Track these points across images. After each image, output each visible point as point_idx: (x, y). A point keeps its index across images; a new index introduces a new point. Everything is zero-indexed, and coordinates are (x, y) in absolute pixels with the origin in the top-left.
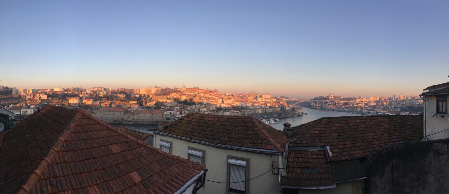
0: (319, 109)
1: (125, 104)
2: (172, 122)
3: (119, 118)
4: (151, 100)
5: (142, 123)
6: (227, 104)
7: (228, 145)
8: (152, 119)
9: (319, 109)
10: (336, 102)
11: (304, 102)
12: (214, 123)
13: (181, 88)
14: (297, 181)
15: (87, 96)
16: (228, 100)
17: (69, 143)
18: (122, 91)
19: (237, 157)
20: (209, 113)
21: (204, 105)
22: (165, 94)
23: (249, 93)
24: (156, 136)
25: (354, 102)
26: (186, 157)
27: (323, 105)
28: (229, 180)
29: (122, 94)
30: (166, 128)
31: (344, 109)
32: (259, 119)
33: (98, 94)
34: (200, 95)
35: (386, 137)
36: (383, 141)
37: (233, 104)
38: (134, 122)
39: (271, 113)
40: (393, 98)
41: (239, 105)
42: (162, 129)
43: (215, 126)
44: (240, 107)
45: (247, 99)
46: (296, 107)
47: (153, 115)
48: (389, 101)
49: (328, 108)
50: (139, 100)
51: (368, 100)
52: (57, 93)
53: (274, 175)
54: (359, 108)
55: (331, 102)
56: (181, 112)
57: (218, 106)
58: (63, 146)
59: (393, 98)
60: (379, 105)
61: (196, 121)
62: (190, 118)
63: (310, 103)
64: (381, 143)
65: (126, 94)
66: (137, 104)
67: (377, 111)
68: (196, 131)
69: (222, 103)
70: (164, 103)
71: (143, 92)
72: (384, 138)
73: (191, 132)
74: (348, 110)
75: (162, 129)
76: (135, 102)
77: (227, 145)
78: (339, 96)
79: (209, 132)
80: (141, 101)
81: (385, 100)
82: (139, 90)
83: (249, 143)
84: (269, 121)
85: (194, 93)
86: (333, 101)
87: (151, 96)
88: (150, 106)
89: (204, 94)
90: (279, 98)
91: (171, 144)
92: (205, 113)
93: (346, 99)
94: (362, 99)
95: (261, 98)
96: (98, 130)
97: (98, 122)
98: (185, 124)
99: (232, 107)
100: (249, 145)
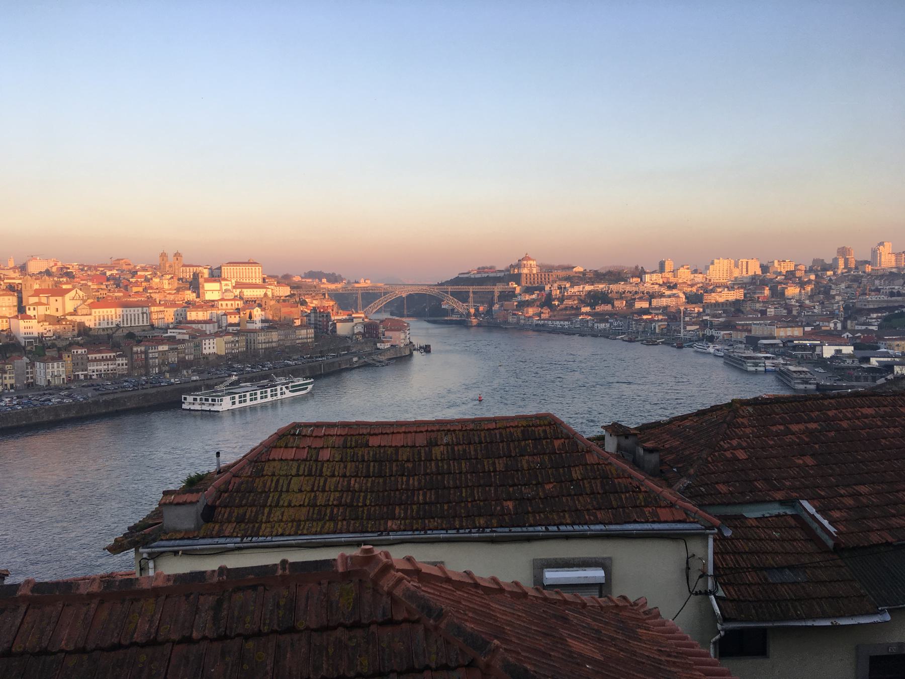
0: (479, 325)
6: (47, 318)
9: (479, 325)
10: (550, 294)
11: (410, 297)
16: (52, 299)
23: (157, 261)
25: (634, 289)
27: (496, 307)
31: (590, 325)
37: (78, 319)
39: (272, 353)
41: (116, 320)
44: (119, 333)
46: (382, 321)
49: (519, 319)
51: (699, 278)
54: (660, 317)
55: (529, 290)
60: (759, 302)
63: (440, 301)
69: (16, 317)
74: (608, 325)
78: (565, 263)
84: (269, 390)
86: (536, 289)
90: (297, 279)
93: (598, 277)
94: (670, 275)
95: (219, 281)
99: (76, 332)
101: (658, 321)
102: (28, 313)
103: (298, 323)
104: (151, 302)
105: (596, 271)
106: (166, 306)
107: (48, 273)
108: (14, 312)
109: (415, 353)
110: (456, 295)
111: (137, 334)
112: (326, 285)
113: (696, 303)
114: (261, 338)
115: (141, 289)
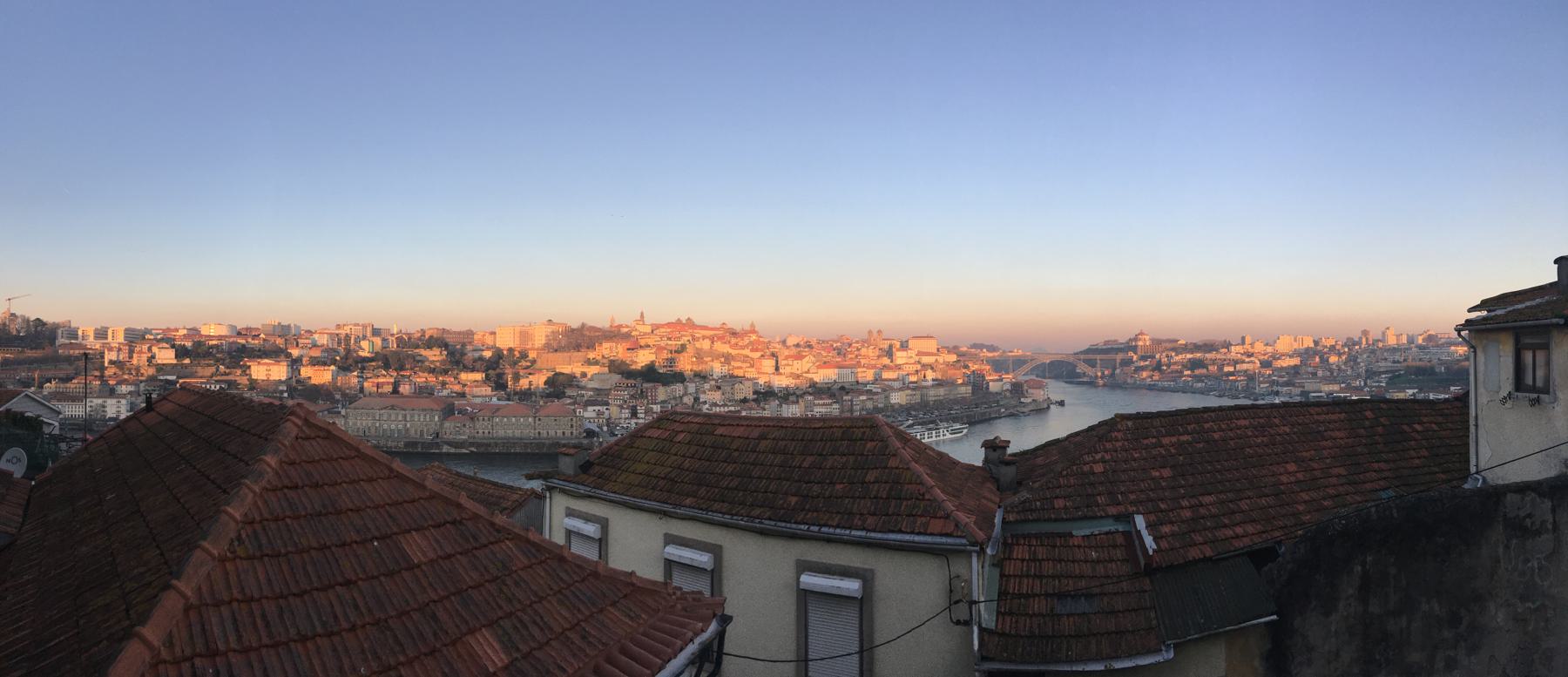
0: (1104, 385)
1: (444, 384)
2: (605, 445)
3: (425, 435)
4: (532, 368)
5: (505, 451)
7: (800, 523)
8: (537, 435)
9: (1104, 385)
10: (1160, 361)
12: (751, 446)
13: (634, 324)
14: (1036, 641)
15: (316, 353)
16: (796, 362)
17: (258, 527)
18: (435, 336)
19: (830, 564)
20: (732, 409)
21: (713, 383)
22: (578, 348)
24: (554, 501)
25: (1224, 357)
26: (655, 573)
27: (1118, 371)
28: (804, 651)
29: (434, 348)
30: (586, 467)
31: (1190, 384)
32: (901, 428)
33: (352, 347)
34: (698, 345)
35: (1339, 476)
36: (1331, 491)
37: (810, 376)
38: (478, 445)
40: (1360, 338)
41: (834, 377)
42: (571, 472)
43: (754, 456)
44: (835, 387)
45: (857, 356)
46: (1026, 381)
47: (539, 420)
48: (1346, 350)
50: (494, 369)
51: (1269, 349)
52: (211, 343)
53: (958, 626)
54: (1242, 378)
56: (636, 407)
57: (762, 383)
58: (239, 538)
59: (1360, 338)
61: (688, 439)
62: (666, 429)
64: (1324, 499)
65: (450, 347)
66: (487, 382)
67: (1304, 387)
68: (691, 476)
69: (774, 373)
70: (575, 377)
71: (505, 341)
72: (1334, 480)
73: (672, 480)
75: (571, 472)
76: (479, 376)
77: (795, 523)
78: (1172, 337)
79: (732, 480)
80: (498, 371)
81: (1333, 348)
82: (493, 333)
83: (869, 514)
84: (934, 432)
85: (679, 338)
87: (532, 355)
88: (530, 389)
89: (713, 343)
91: (604, 524)
92: (718, 409)
93: (1196, 348)
96: (357, 479)
97: (357, 450)
98: (650, 454)
100: (870, 520)
101: (1240, 381)
102: (781, 371)
103: (960, 381)
104: (859, 365)
105: (1195, 344)
106: (867, 368)
107: (798, 345)
108: (772, 370)
109: (1052, 406)
110: (1087, 361)
111: (847, 387)
112: (986, 354)
113: (1268, 367)
114: (932, 392)
115: (853, 356)
